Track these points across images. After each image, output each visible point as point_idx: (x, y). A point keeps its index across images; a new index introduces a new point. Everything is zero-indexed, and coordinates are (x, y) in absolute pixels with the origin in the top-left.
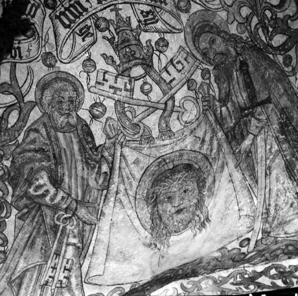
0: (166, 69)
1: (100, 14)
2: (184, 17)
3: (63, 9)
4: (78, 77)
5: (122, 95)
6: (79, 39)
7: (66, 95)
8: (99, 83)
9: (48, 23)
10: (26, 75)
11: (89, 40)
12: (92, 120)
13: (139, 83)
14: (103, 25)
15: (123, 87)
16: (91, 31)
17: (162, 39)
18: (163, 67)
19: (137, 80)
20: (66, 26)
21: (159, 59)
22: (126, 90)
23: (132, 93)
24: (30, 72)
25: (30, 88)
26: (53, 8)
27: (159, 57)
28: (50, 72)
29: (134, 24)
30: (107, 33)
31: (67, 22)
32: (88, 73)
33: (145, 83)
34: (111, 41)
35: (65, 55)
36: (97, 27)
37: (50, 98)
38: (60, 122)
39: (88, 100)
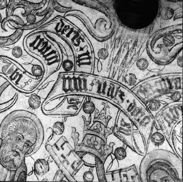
0: (113, 173)
1: (92, 100)
2: (152, 146)
3: (71, 76)
4: (45, 130)
5: (68, 170)
6: (66, 104)
7: (28, 137)
8: (57, 147)
9: (54, 77)
10: (10, 99)
11: (72, 110)
12: (32, 171)
13: (87, 169)
14: (88, 108)
15: (71, 163)
16: (78, 106)
17: (124, 150)
18: (111, 170)
19: (86, 165)
20: (64, 89)
21: (112, 162)
22: (73, 167)
23: (75, 172)
24: (15, 99)
25: (4, 111)
26: (67, 70)
27: (113, 160)
28: (29, 110)
29: (111, 124)
30: (87, 116)
31: (67, 87)
32: (53, 132)
33: (90, 172)
34: (87, 123)
35: (47, 107)
36: (84, 106)
37: (14, 130)
38: (7, 155)
39: (40, 153)
